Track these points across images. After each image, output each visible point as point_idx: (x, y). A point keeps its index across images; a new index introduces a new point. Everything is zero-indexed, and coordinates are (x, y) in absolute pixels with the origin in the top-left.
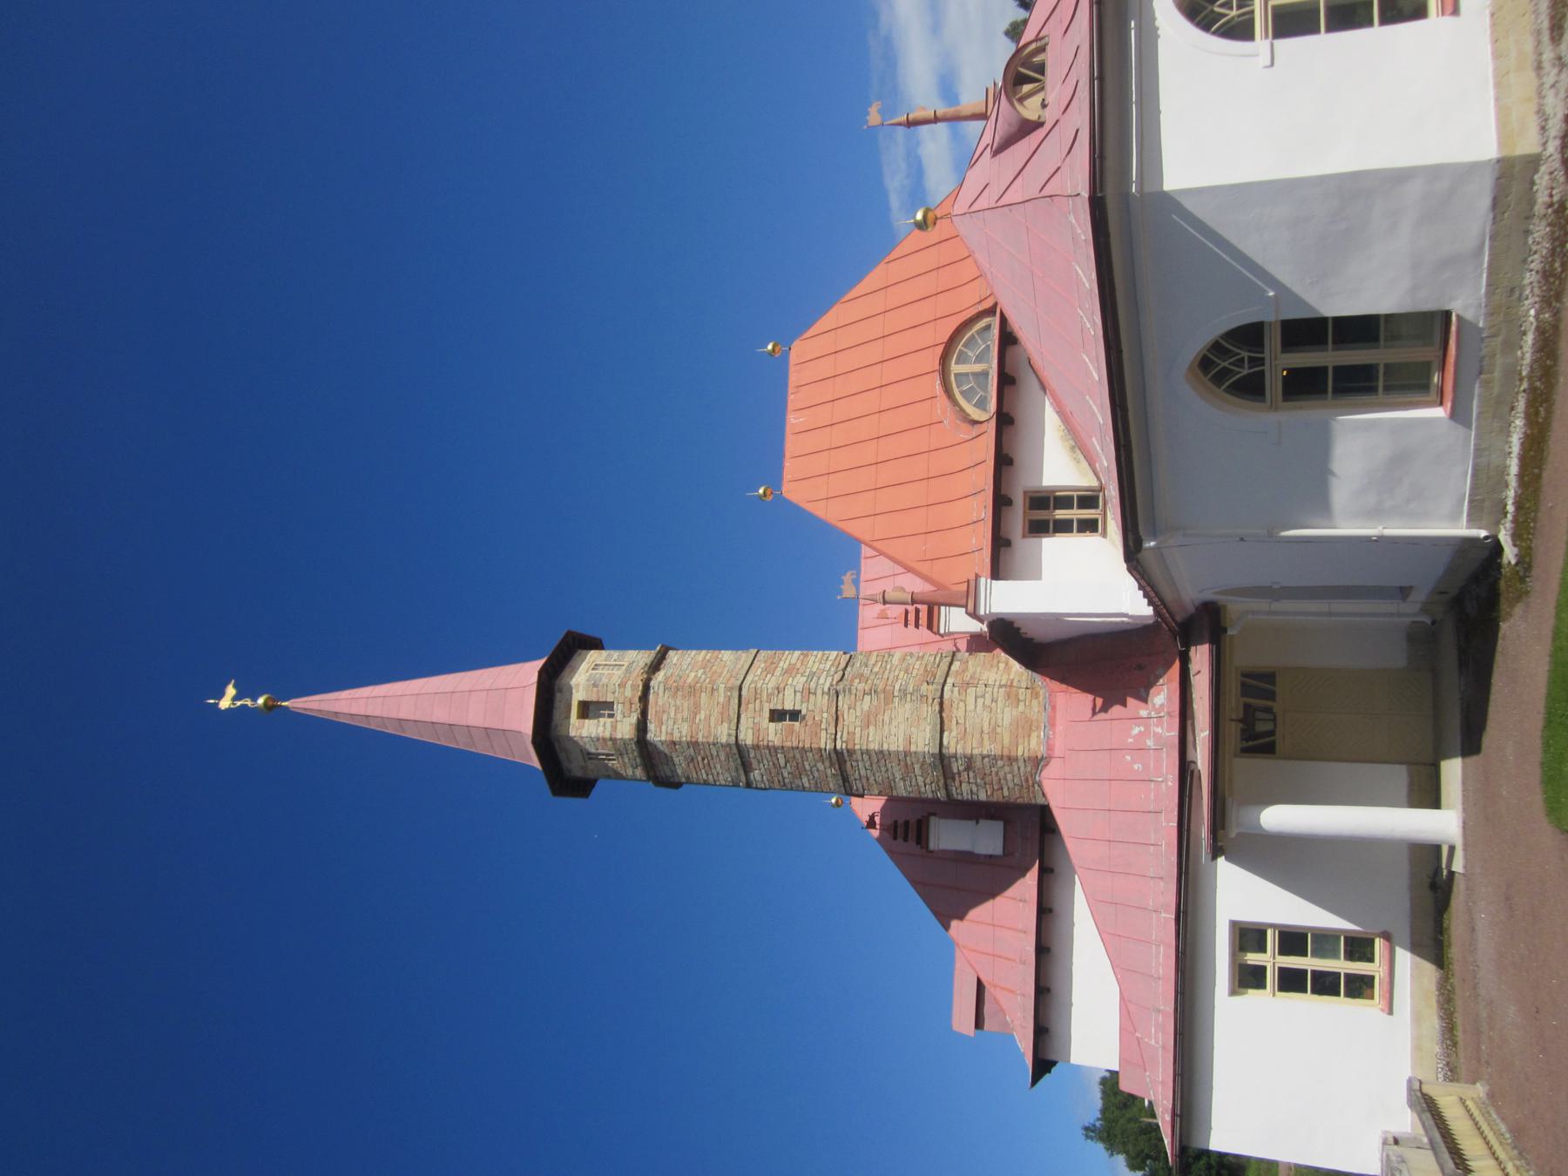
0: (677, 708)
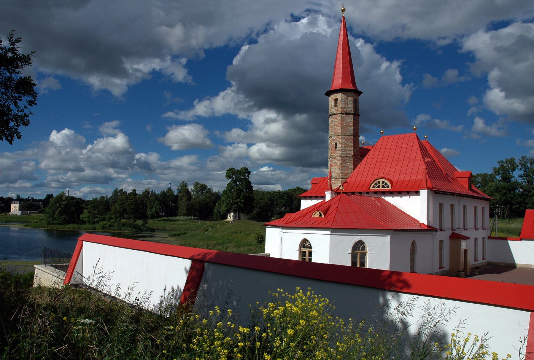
0: (337, 122)
